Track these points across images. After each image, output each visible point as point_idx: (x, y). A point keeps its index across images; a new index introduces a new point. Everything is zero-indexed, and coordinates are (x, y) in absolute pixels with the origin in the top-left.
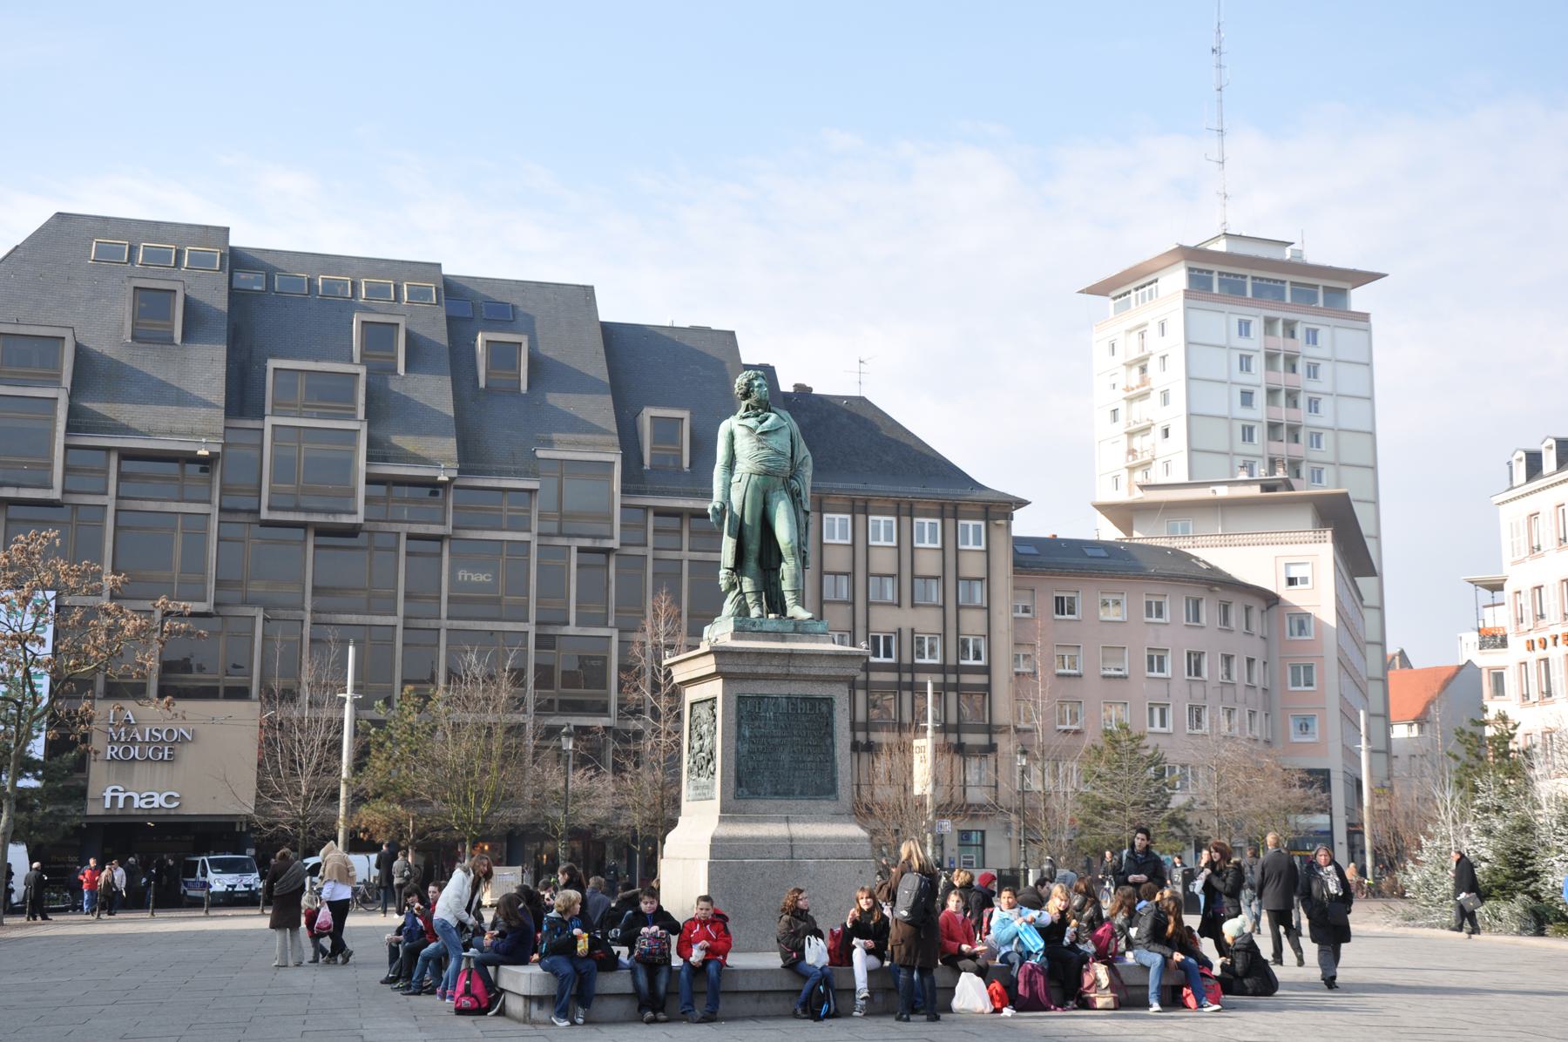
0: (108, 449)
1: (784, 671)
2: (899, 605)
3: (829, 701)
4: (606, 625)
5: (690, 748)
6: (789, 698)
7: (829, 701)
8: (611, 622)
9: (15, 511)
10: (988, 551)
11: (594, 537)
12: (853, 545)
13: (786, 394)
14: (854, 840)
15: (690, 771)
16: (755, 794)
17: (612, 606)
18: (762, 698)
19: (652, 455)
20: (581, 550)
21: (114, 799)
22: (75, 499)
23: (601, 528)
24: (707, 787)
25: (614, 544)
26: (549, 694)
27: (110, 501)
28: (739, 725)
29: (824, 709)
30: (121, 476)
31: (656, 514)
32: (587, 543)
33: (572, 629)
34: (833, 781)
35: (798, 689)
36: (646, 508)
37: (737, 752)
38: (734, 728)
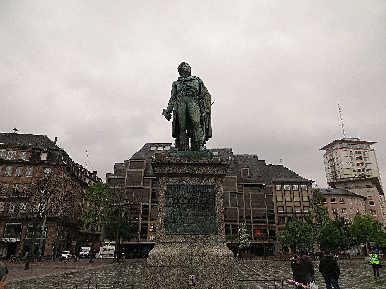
0: (150, 179)
1: (189, 172)
2: (291, 201)
3: (212, 186)
4: (236, 206)
7: (212, 186)
8: (237, 206)
9: (136, 190)
10: (307, 191)
11: (233, 190)
12: (282, 191)
13: (268, 166)
14: (226, 256)
16: (175, 233)
17: (237, 203)
20: (231, 193)
21: (151, 238)
22: (145, 187)
23: (235, 189)
25: (237, 191)
26: (226, 219)
27: (150, 187)
28: (167, 199)
29: (210, 190)
30: (152, 183)
32: (232, 191)
33: (230, 207)
34: (216, 226)
35: (197, 181)
37: (166, 211)
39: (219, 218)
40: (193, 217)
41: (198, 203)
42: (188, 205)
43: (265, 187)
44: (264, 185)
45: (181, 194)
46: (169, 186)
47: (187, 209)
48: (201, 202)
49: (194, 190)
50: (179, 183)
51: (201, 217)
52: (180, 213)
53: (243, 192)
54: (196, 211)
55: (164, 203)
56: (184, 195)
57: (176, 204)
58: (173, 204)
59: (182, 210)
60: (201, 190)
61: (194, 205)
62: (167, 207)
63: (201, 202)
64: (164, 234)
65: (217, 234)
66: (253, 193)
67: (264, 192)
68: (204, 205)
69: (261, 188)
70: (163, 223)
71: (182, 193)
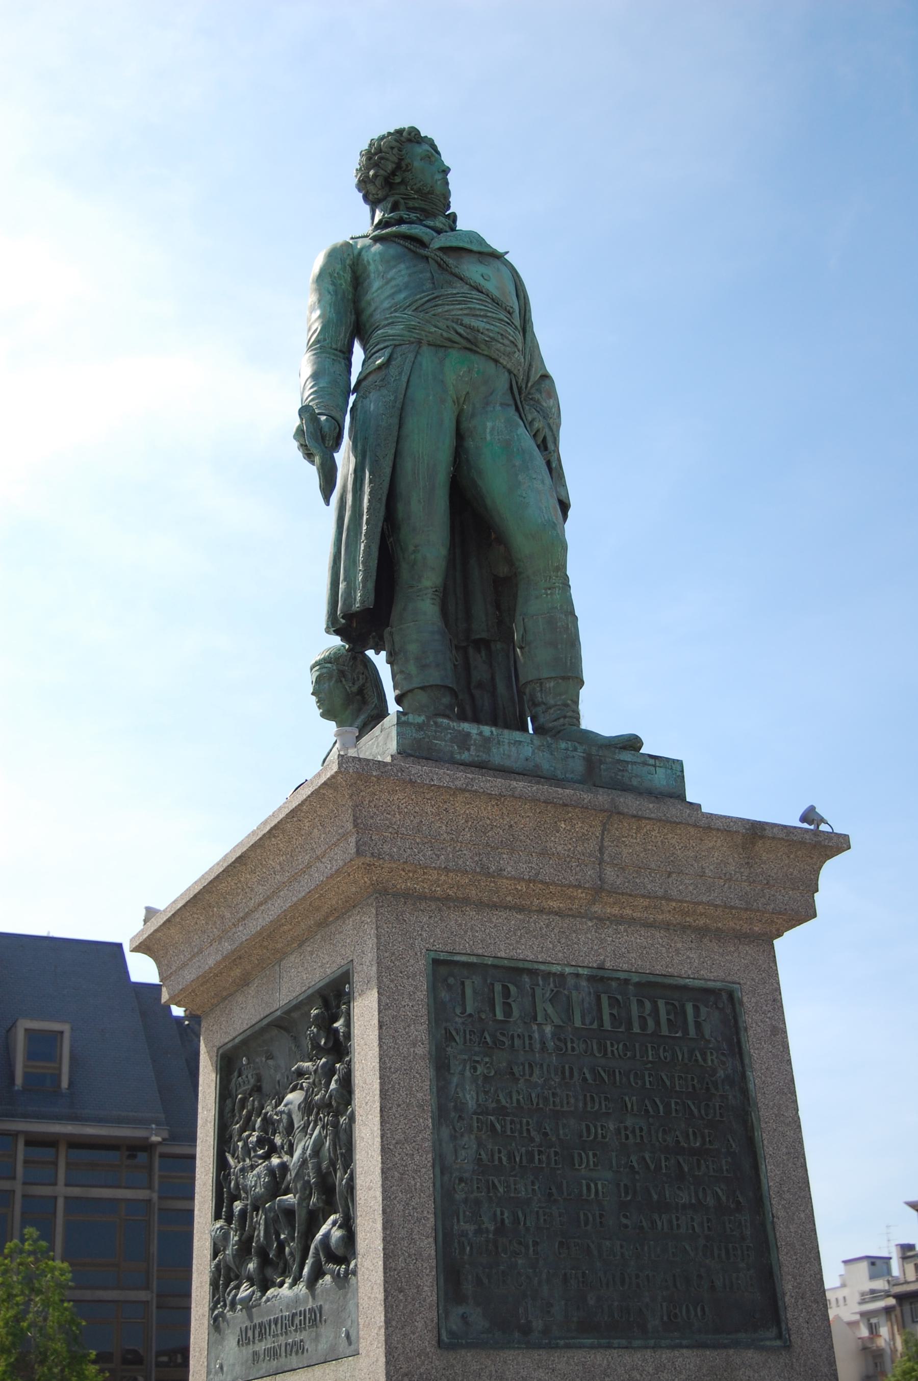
5: (224, 1196)
6: (599, 979)
15: (224, 1279)
18: (514, 972)
19: (26, 1075)
24: (314, 1318)
28: (441, 1065)
31: (28, 1143)
36: (15, 1135)
37: (441, 1164)
38: (424, 1072)
39: (787, 1227)
40: (626, 1217)
41: (647, 1111)
42: (588, 1127)
43: (162, 1156)
44: (155, 1139)
45: (530, 1038)
46: (443, 970)
47: (580, 1156)
48: (667, 1106)
49: (611, 1014)
50: (513, 953)
51: (678, 1219)
52: (533, 1183)
53: (14, 1178)
54: (638, 1173)
55: (419, 1095)
56: (551, 1044)
57: (501, 1111)
58: (482, 1111)
59: (548, 1157)
60: (658, 1023)
61: (626, 1128)
62: (445, 1132)
63: (667, 1106)
64: (440, 1344)
65: (788, 1347)
66: (76, 1191)
67: (150, 1187)
68: (688, 1135)
69: (129, 1157)
70: (425, 1254)
71: (535, 1027)
